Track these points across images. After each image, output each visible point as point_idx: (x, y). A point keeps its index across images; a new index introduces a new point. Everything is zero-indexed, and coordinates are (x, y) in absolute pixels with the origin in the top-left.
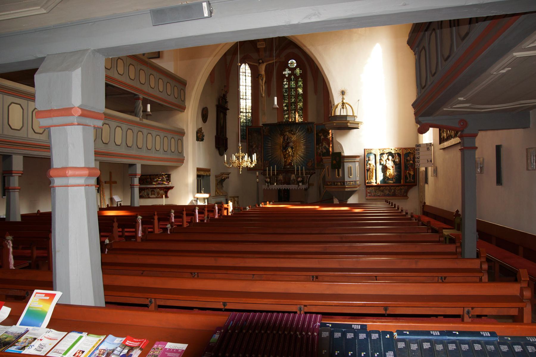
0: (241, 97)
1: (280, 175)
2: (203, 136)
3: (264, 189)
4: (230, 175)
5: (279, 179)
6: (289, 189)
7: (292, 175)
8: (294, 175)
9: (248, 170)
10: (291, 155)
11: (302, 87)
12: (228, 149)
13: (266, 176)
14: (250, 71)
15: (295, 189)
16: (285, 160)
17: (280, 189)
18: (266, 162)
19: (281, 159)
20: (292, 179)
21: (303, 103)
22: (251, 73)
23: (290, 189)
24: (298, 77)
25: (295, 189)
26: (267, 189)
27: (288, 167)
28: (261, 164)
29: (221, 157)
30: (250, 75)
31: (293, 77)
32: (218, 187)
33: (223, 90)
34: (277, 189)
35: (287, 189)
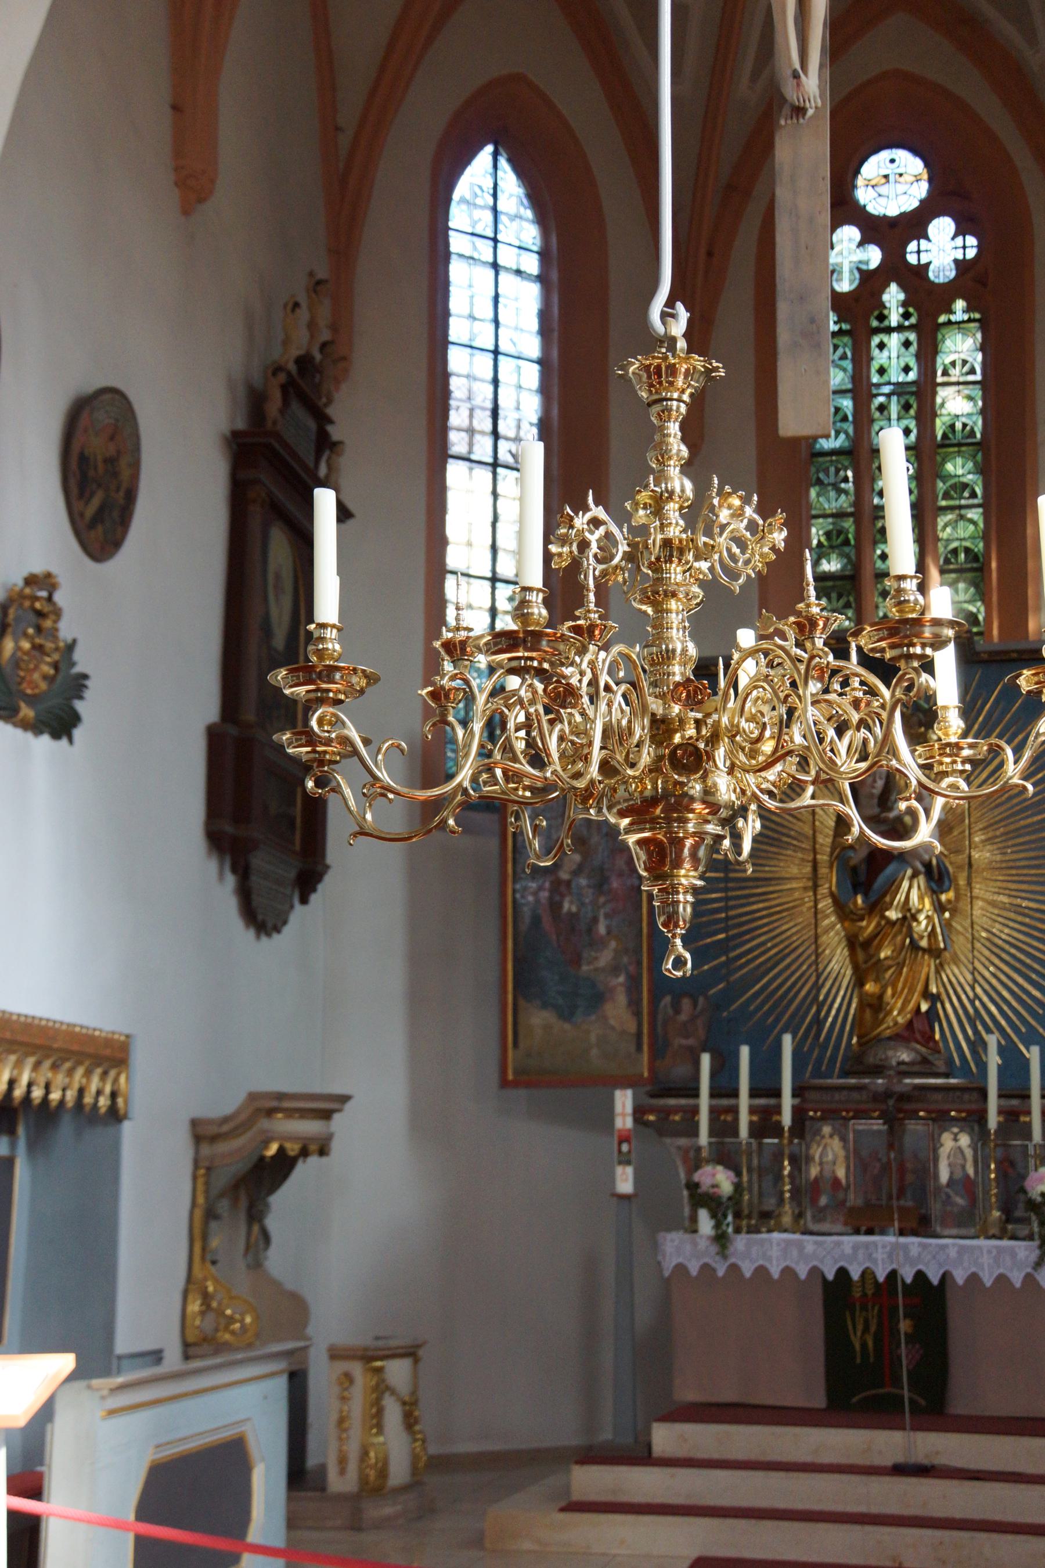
0: (457, 442)
1: (827, 1130)
2: (78, 685)
3: (681, 1268)
4: (336, 1116)
5: (814, 1171)
6: (935, 1280)
7: (947, 1142)
8: (965, 1140)
9: (504, 1083)
10: (924, 943)
11: (978, 377)
12: (328, 879)
13: (683, 1141)
14: (530, 234)
15: (1002, 1280)
16: (869, 987)
17: (842, 1273)
18: (677, 1011)
19: (817, 987)
20: (944, 1176)
21: (986, 516)
22: (544, 255)
23: (945, 1277)
24: (944, 295)
25: (1002, 1280)
26: (706, 1268)
27: (905, 1056)
28: (632, 1027)
29: (264, 939)
30: (532, 264)
31: (893, 296)
32: (214, 1243)
33: (296, 305)
34: (815, 1271)
35: (920, 1276)
